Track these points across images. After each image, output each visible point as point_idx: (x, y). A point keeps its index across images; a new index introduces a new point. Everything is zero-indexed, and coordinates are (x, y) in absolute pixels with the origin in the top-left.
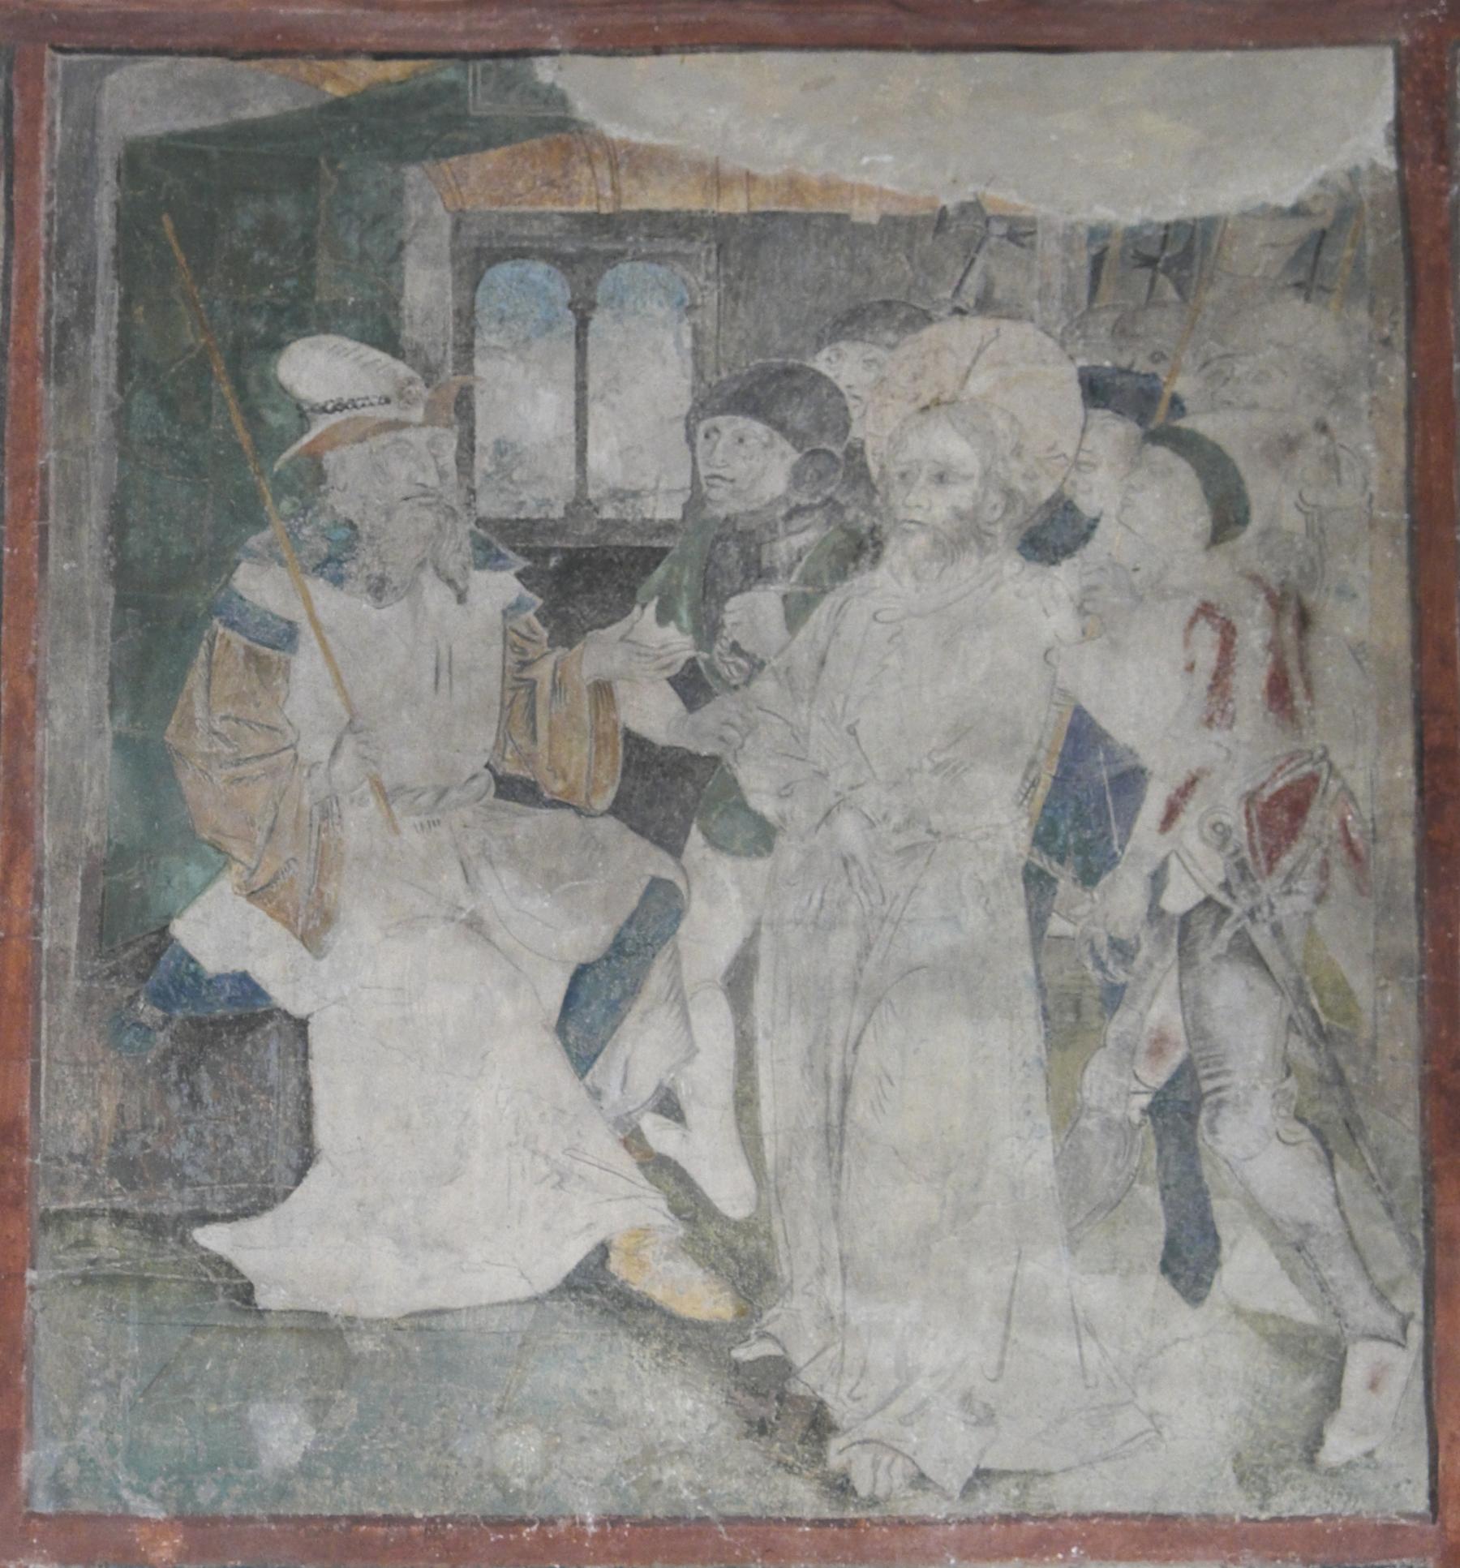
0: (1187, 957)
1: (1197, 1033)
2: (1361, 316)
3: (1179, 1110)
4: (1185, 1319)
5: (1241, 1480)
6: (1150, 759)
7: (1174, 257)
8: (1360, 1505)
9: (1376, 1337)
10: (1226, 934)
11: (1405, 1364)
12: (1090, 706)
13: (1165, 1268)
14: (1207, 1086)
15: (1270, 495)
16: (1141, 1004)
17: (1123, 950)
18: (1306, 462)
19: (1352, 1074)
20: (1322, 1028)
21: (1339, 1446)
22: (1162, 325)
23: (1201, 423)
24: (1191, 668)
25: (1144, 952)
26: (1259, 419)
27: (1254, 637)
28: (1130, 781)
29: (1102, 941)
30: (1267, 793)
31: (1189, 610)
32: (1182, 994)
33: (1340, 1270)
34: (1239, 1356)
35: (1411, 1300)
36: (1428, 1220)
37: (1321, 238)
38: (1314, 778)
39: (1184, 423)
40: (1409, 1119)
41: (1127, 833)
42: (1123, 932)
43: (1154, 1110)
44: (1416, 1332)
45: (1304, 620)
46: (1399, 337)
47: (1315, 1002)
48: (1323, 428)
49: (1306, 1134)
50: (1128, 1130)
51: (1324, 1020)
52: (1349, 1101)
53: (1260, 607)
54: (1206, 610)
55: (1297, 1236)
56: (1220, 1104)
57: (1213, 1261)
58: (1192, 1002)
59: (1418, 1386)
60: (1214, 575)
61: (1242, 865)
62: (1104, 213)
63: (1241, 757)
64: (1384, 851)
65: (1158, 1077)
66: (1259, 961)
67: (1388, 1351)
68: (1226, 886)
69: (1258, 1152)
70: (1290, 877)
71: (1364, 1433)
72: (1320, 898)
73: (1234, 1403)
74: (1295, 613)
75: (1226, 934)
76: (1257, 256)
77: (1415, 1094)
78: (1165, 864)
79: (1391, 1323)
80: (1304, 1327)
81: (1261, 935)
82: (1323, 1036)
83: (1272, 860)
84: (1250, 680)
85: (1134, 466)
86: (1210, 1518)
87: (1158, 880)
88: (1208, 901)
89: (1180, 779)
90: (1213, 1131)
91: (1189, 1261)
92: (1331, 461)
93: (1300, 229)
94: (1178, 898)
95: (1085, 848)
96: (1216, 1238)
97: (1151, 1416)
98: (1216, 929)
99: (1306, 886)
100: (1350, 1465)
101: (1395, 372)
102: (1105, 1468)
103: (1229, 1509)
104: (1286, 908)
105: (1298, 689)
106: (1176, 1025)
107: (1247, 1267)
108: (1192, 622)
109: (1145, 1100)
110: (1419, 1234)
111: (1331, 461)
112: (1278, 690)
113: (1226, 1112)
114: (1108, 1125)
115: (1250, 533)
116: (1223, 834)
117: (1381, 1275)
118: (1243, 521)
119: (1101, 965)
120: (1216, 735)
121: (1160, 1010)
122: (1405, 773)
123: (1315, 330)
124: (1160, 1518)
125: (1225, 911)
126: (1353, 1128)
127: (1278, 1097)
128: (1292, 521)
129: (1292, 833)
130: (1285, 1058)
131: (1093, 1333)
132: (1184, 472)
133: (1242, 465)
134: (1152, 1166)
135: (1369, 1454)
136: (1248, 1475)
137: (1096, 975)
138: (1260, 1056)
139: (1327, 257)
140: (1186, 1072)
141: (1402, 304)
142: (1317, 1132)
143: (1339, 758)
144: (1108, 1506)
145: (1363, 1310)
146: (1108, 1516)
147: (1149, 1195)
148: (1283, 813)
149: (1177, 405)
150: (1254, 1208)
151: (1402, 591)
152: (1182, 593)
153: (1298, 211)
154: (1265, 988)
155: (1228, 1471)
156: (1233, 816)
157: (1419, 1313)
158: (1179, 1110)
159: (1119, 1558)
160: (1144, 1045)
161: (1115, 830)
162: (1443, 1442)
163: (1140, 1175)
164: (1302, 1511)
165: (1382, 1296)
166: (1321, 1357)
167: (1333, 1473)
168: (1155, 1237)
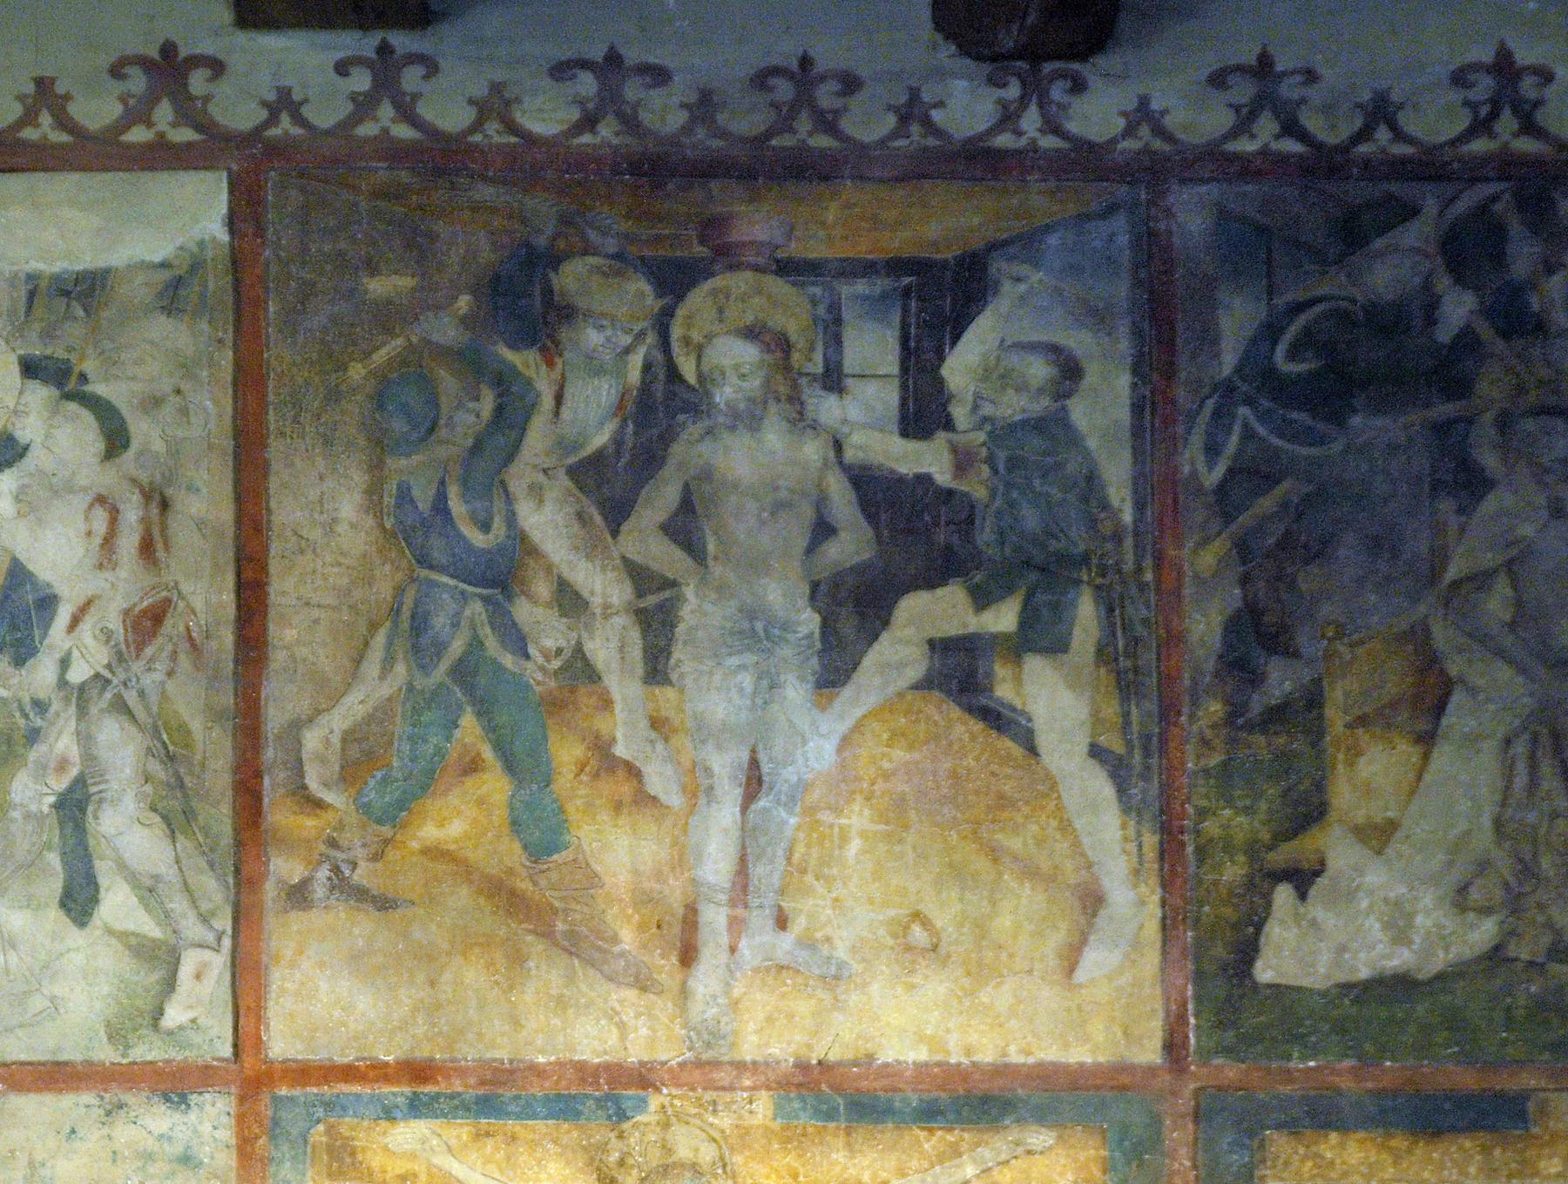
0: (82, 712)
1: (88, 757)
2: (205, 326)
3: (74, 807)
4: (76, 938)
5: (110, 1038)
6: (62, 589)
7: (85, 290)
8: (187, 1053)
9: (200, 946)
10: (108, 695)
11: (219, 962)
12: (22, 558)
13: (63, 905)
14: (93, 789)
15: (144, 431)
16: (52, 739)
17: (40, 706)
18: (168, 411)
19: (188, 780)
20: (169, 750)
21: (175, 1015)
22: (74, 331)
23: (99, 389)
24: (89, 534)
25: (53, 709)
26: (137, 387)
27: (132, 514)
28: (48, 603)
29: (27, 700)
30: (137, 609)
31: (89, 499)
32: (78, 733)
33: (178, 904)
34: (111, 961)
35: (224, 922)
36: (237, 871)
37: (177, 283)
38: (168, 601)
39: (88, 388)
40: (226, 809)
41: (45, 635)
42: (42, 695)
43: (59, 806)
44: (227, 942)
45: (165, 505)
46: (229, 337)
47: (165, 736)
48: (178, 392)
49: (158, 819)
50: (40, 818)
51: (171, 748)
52: (185, 796)
53: (136, 498)
54: (101, 500)
55: (149, 883)
56: (101, 801)
57: (94, 900)
58: (85, 739)
59: (228, 977)
60: (107, 478)
61: (119, 654)
62: (41, 266)
63: (123, 588)
64: (214, 644)
65: (61, 784)
66: (132, 717)
67: (207, 955)
68: (109, 666)
69: (127, 832)
70: (152, 660)
71: (191, 1007)
72: (170, 674)
73: (106, 989)
74: (159, 501)
75: (108, 695)
76: (139, 290)
77: (229, 793)
78: (69, 653)
79: (211, 938)
80: (154, 940)
81: (131, 698)
82: (171, 758)
83: (140, 648)
84: (128, 542)
85: (54, 412)
86: (88, 1063)
87: (65, 663)
88: (97, 676)
89: (81, 601)
90: (96, 818)
91: (79, 900)
92: (184, 411)
93: (166, 275)
94: (78, 673)
95: (18, 643)
96: (96, 884)
97: (53, 999)
98: (101, 693)
99: (161, 666)
100: (181, 1028)
101: (226, 358)
102: (19, 1032)
103: (102, 1057)
104: (148, 680)
105: (159, 546)
106: (74, 753)
107: (118, 904)
108: (91, 505)
109: (52, 799)
110: (231, 881)
111: (184, 411)
112: (147, 548)
113: (104, 806)
114: (28, 816)
115: (131, 453)
116: (108, 635)
117: (205, 906)
118: (126, 445)
119: (26, 716)
120: (107, 575)
121: (63, 742)
122: (228, 597)
123: (173, 335)
124: (58, 1064)
125: (108, 682)
126: (189, 814)
127: (140, 796)
128: (158, 446)
129: (154, 634)
130: (145, 771)
131: (13, 947)
132: (87, 417)
133: (125, 412)
134: (56, 840)
135: (193, 1021)
136: (116, 1035)
137: (22, 722)
138: (128, 771)
139: (182, 292)
140: (80, 782)
141: (231, 318)
142: (165, 818)
143: (186, 587)
144: (23, 1057)
145: (192, 928)
146: (23, 1064)
147: (54, 859)
148: (148, 622)
149: (83, 378)
150: (122, 867)
151: (228, 488)
152: (84, 489)
153: (164, 265)
154: (133, 730)
155: (102, 1033)
156: (115, 623)
157: (229, 932)
158: (74, 807)
159: (29, 1090)
160: (52, 765)
161: (36, 632)
162: (242, 1012)
163: (48, 846)
164: (149, 1058)
165: (205, 919)
166: (162, 959)
167: (170, 1033)
168: (56, 885)
